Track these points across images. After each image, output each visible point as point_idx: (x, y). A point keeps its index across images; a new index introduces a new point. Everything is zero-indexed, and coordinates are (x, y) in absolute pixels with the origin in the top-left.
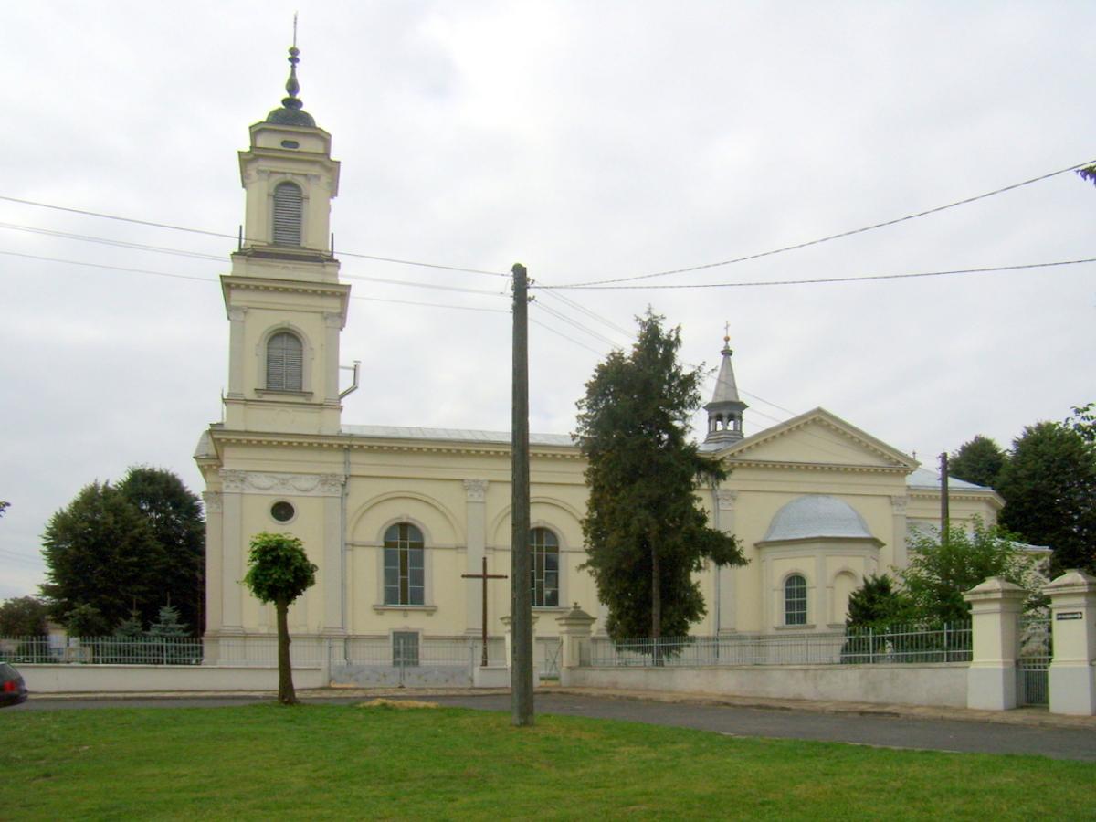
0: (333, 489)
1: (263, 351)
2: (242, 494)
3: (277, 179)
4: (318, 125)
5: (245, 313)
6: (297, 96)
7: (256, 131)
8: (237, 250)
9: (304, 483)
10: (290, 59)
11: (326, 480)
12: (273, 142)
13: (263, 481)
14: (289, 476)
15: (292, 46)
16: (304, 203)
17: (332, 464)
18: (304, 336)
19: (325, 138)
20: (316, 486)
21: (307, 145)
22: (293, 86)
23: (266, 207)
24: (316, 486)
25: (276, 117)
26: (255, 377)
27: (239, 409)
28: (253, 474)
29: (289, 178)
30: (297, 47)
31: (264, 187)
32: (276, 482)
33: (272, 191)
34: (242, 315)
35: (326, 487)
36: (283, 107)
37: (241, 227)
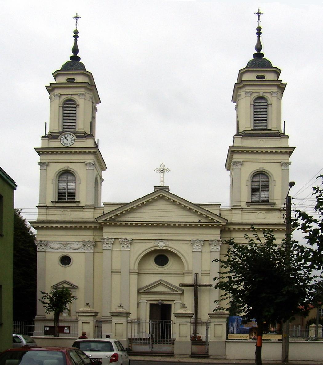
0: (89, 248)
1: (56, 182)
2: (46, 252)
3: (64, 98)
4: (87, 70)
5: (47, 165)
6: (78, 55)
7: (56, 75)
8: (44, 135)
9: (75, 246)
10: (74, 36)
11: (85, 244)
12: (62, 79)
13: (56, 245)
14: (67, 243)
15: (75, 29)
16: (77, 108)
17: (88, 236)
18: (77, 174)
19: (89, 76)
20: (81, 247)
21: (79, 79)
22: (75, 50)
23: (58, 112)
24: (81, 247)
25: (66, 67)
26: (51, 195)
27: (44, 210)
28: (51, 242)
29: (69, 97)
30: (78, 30)
31: (58, 102)
32: (62, 245)
33: (61, 104)
34: (46, 166)
35: (86, 248)
36: (70, 60)
37: (46, 123)
